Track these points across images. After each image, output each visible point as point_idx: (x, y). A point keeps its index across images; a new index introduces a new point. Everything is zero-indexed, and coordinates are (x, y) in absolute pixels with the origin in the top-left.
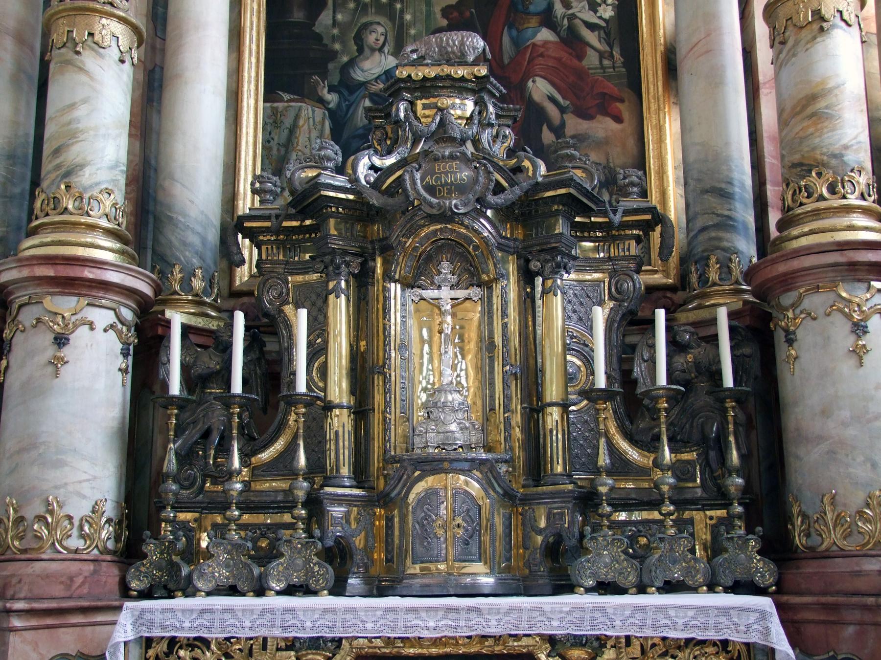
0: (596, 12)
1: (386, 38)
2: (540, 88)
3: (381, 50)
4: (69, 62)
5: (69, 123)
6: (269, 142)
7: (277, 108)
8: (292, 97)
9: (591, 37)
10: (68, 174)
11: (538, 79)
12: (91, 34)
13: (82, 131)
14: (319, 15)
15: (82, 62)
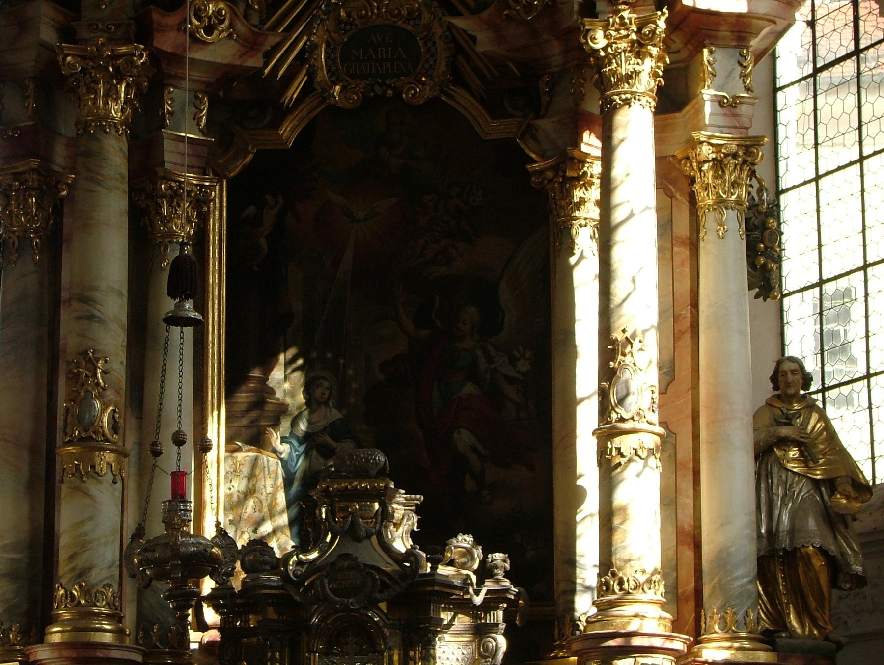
0: (514, 366)
1: (330, 393)
2: (464, 438)
3: (326, 403)
8: (249, 447)
9: (511, 391)
11: (462, 431)
12: (93, 467)
14: (272, 369)
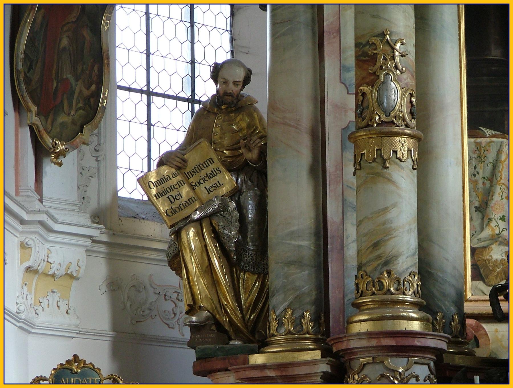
4: (379, 175)
5: (384, 223)
6: (475, 175)
7: (480, 143)
8: (494, 132)
10: (386, 263)
12: (395, 152)
13: (395, 230)
15: (389, 174)
